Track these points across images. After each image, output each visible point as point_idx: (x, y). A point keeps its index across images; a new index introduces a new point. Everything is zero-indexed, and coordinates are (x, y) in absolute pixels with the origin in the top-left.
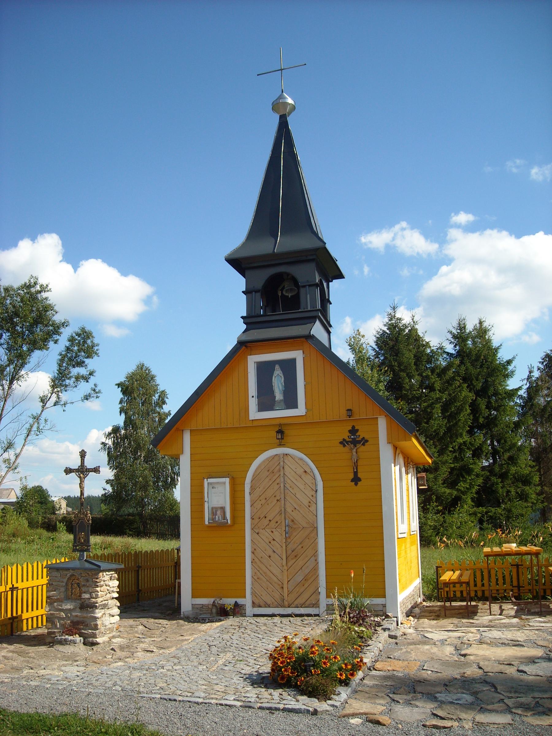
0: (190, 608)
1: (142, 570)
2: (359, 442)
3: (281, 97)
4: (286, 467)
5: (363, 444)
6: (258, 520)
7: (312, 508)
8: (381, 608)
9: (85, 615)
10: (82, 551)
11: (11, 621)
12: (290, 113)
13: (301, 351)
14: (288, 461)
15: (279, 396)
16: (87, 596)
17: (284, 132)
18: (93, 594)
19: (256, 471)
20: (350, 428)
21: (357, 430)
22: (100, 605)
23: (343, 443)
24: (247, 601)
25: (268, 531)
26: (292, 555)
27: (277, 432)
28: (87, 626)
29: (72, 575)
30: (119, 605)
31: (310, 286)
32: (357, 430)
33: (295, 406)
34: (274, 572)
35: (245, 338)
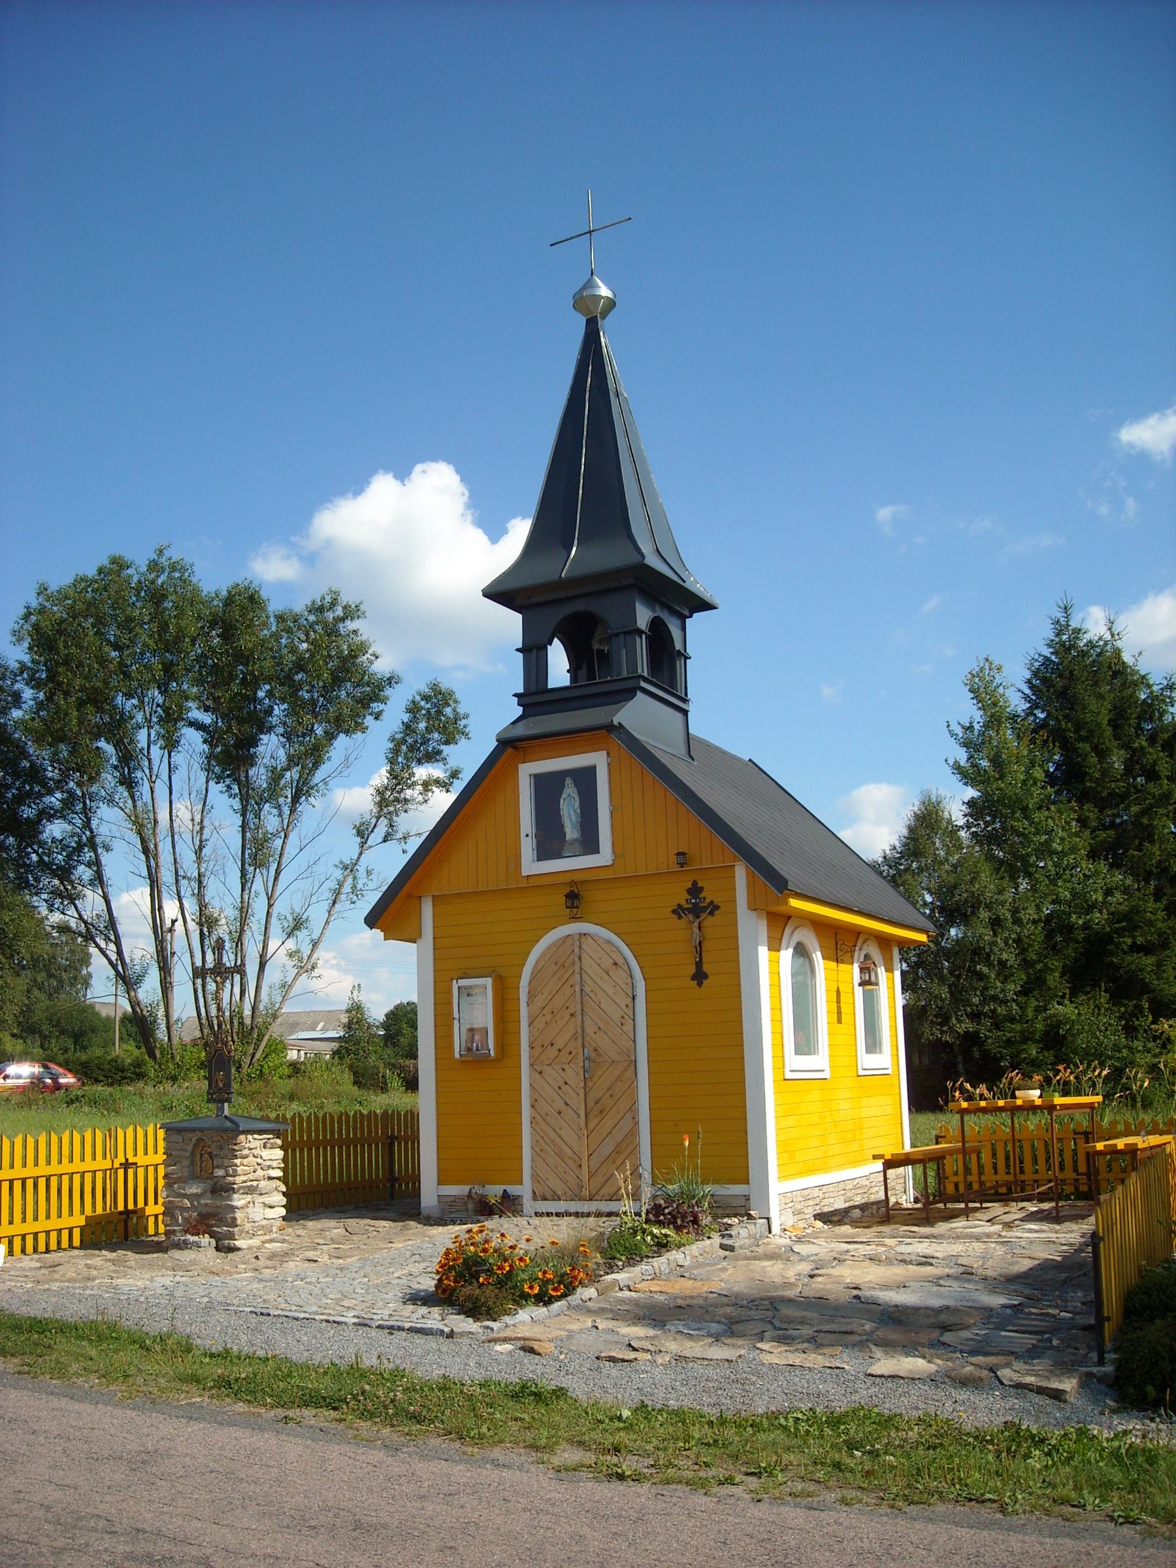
0: (435, 1202)
1: (399, 1144)
2: (704, 909)
3: (589, 284)
4: (584, 956)
5: (711, 913)
6: (539, 1049)
7: (628, 1027)
8: (742, 1202)
9: (218, 1203)
10: (222, 1101)
11: (124, 1217)
12: (604, 315)
13: (605, 753)
14: (588, 944)
15: (571, 832)
16: (220, 1172)
17: (591, 352)
18: (228, 1167)
19: (537, 963)
20: (689, 885)
21: (702, 888)
22: (240, 1188)
23: (678, 911)
24: (524, 1190)
25: (557, 1067)
26: (594, 1110)
27: (567, 896)
28: (222, 1221)
29: (200, 1140)
30: (284, 1189)
31: (626, 633)
32: (702, 888)
33: (596, 850)
34: (566, 1138)
35: (521, 731)
